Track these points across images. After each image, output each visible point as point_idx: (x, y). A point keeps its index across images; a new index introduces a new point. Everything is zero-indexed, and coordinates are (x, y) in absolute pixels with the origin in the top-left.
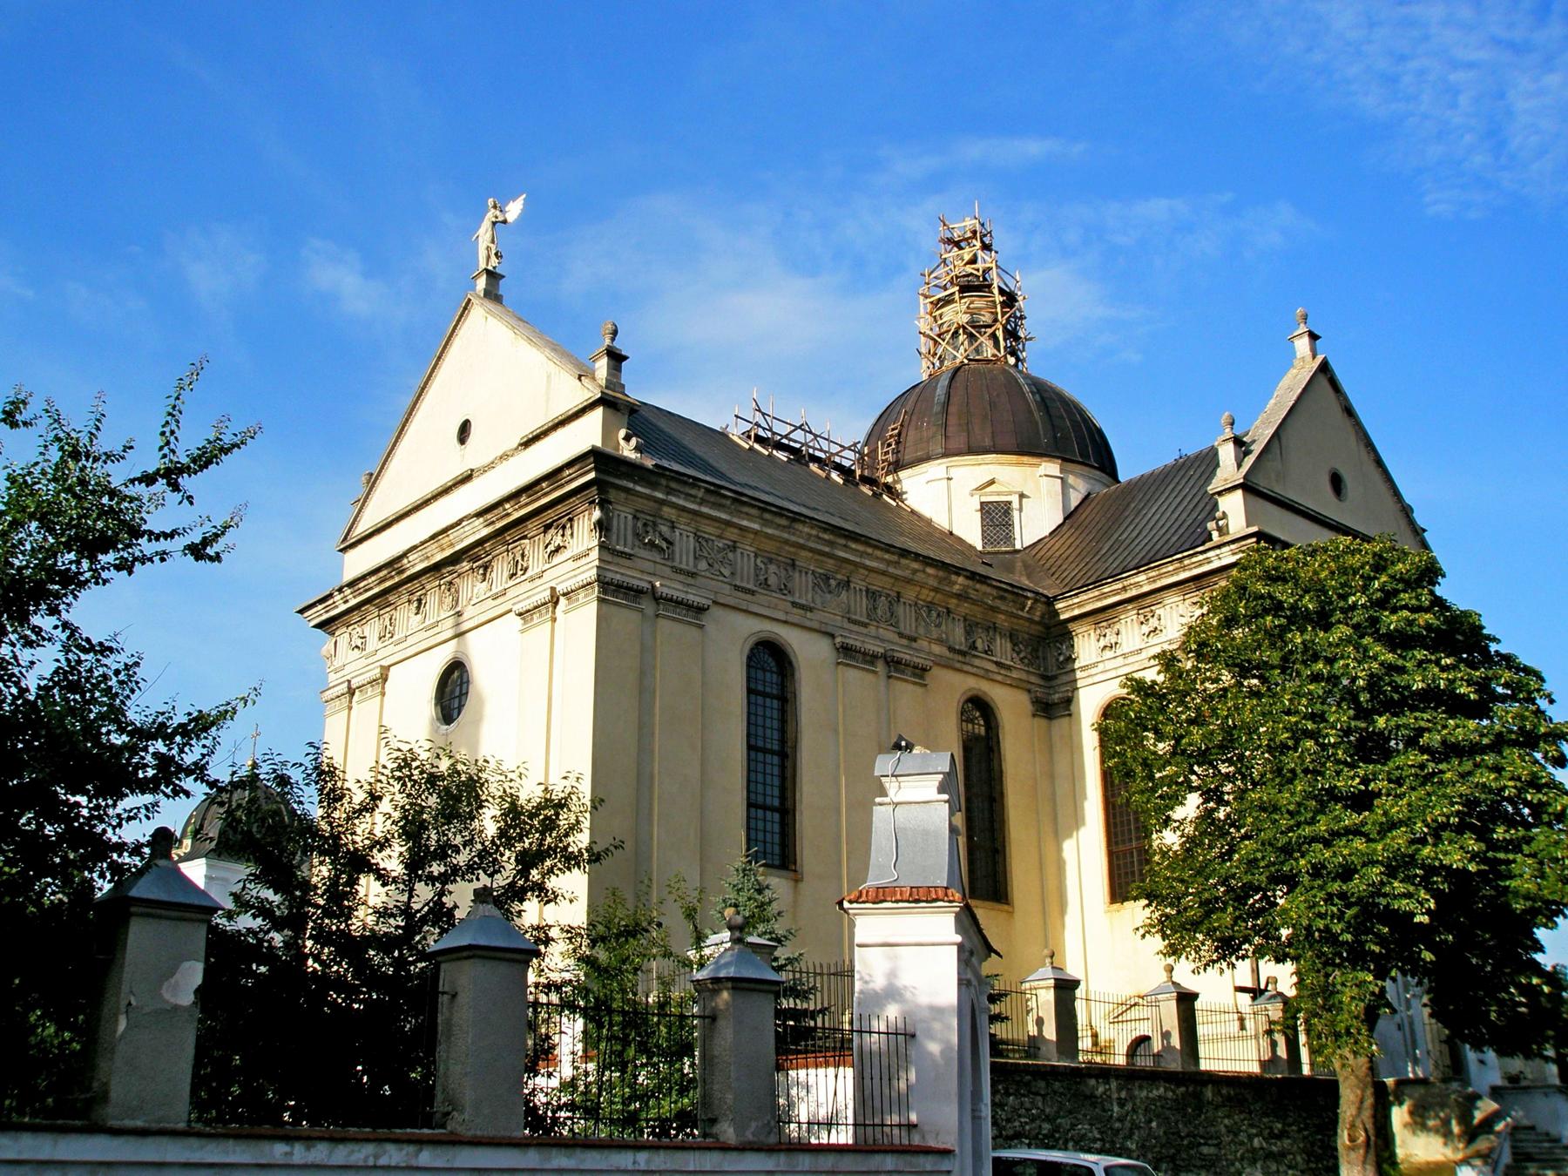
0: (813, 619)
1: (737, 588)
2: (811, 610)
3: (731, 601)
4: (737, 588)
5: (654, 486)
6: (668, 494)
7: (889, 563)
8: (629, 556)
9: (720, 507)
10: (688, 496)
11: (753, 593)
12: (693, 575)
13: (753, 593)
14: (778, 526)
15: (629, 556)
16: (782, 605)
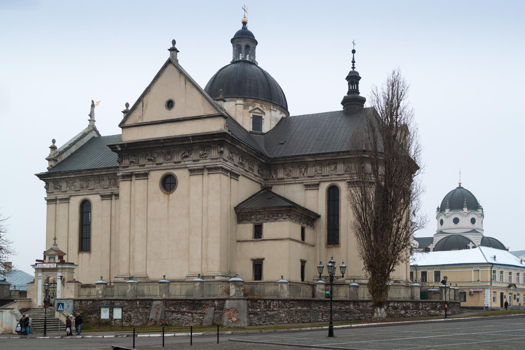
0: (94, 191)
1: (76, 191)
2: (94, 189)
3: (75, 194)
4: (76, 191)
5: (50, 177)
6: (54, 176)
7: (107, 171)
8: (52, 193)
9: (65, 175)
10: (58, 176)
11: (79, 190)
12: (66, 191)
13: (79, 190)
14: (78, 174)
15: (52, 193)
16: (86, 191)
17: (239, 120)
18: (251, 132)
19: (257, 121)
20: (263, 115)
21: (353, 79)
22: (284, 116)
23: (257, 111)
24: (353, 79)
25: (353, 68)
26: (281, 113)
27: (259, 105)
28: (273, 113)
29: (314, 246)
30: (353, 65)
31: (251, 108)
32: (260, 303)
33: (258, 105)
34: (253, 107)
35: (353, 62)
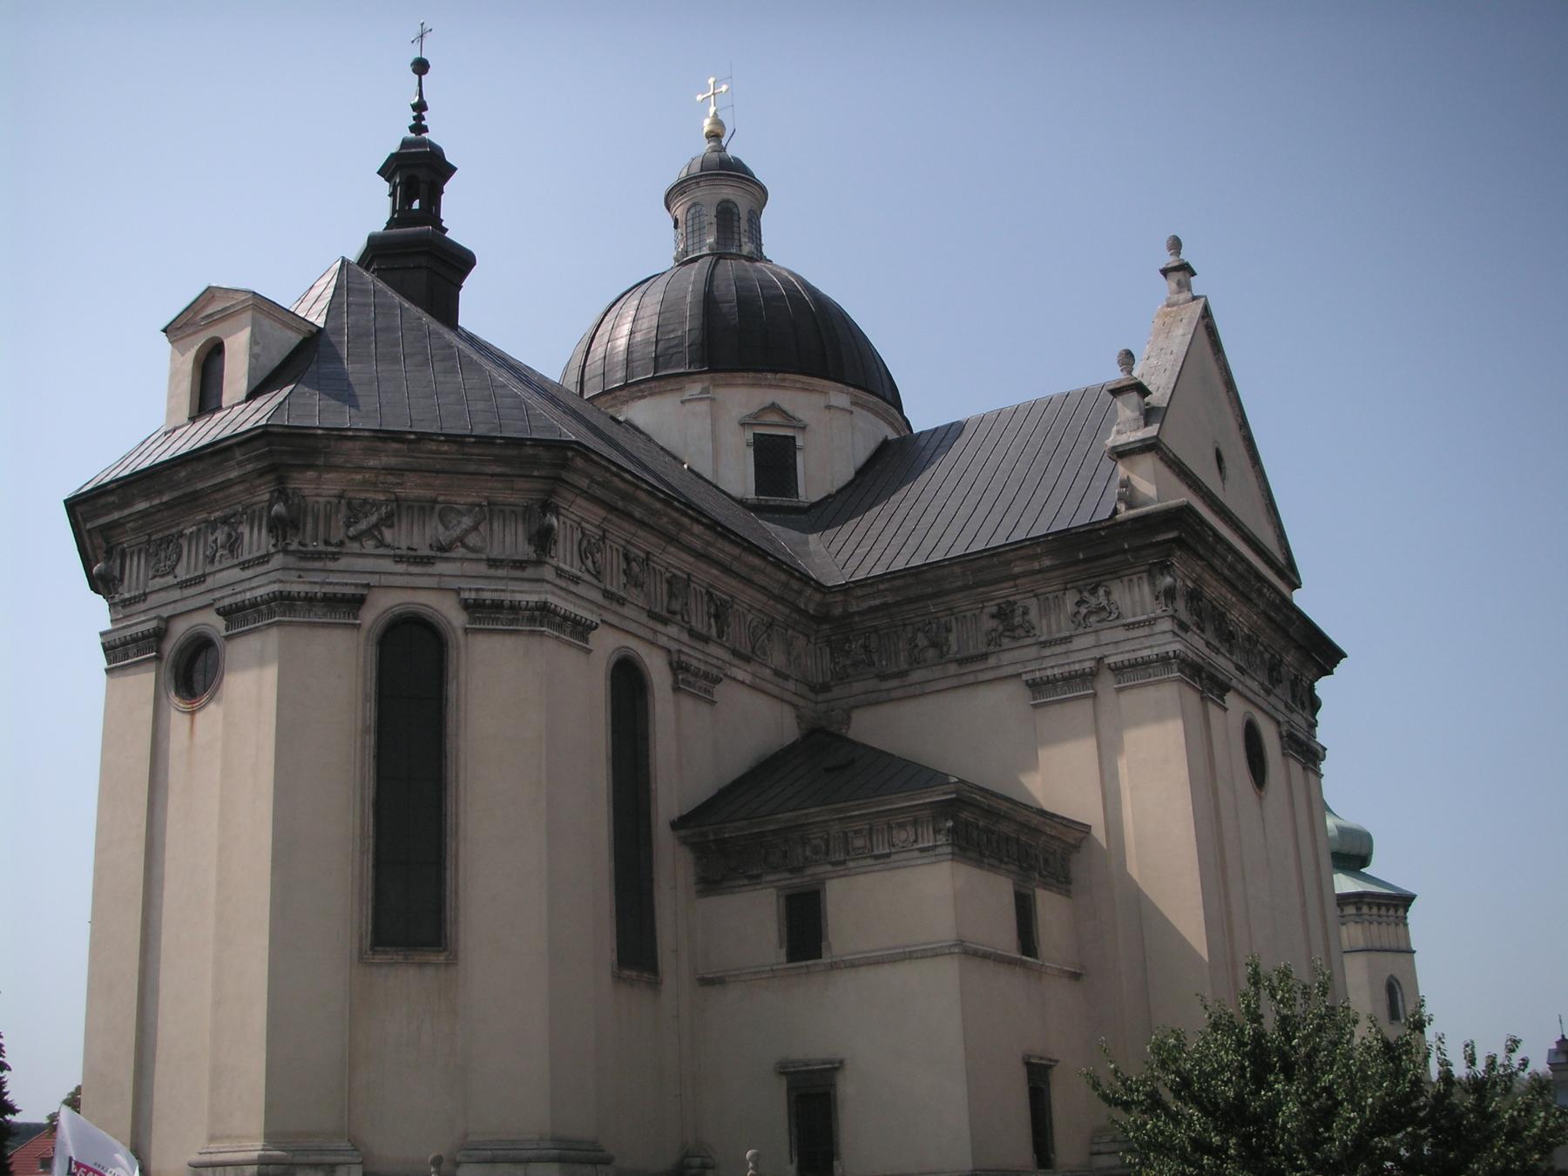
21: (418, 172)
24: (418, 172)
25: (419, 128)
30: (419, 118)
35: (420, 107)
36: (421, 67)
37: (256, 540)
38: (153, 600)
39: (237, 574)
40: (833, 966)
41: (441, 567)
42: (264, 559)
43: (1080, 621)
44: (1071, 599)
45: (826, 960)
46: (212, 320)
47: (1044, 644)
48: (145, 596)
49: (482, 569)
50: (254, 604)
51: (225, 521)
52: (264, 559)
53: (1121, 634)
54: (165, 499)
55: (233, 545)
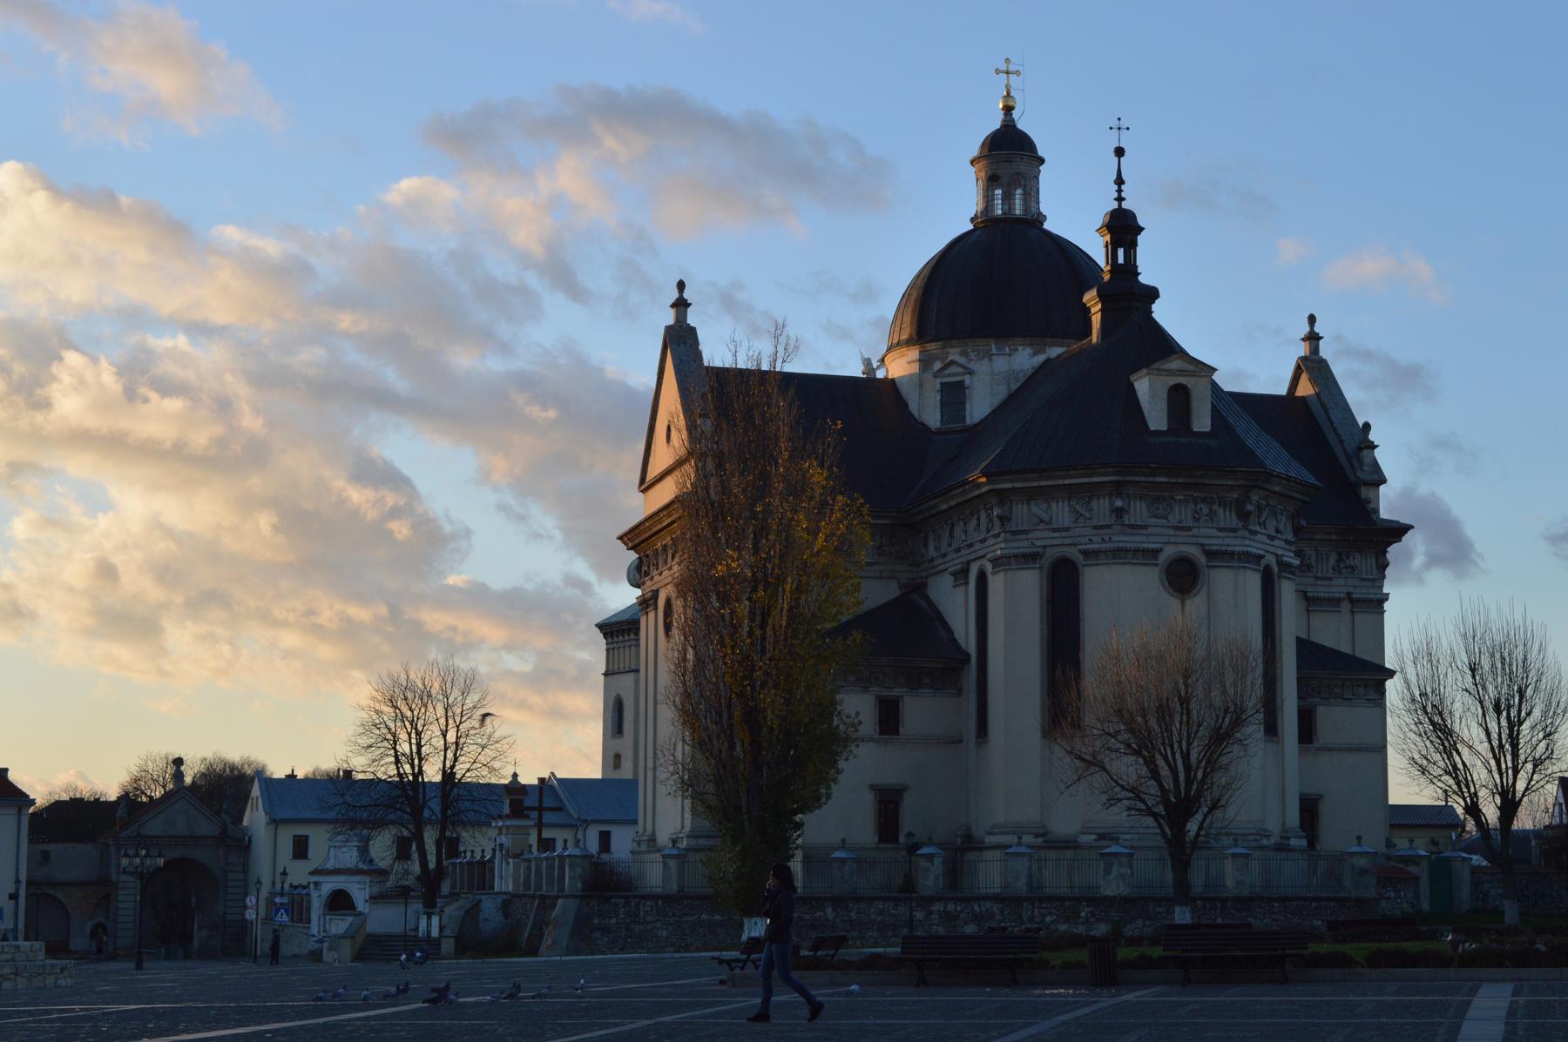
17: (914, 408)
18: (939, 432)
19: (954, 396)
20: (967, 379)
22: (1055, 352)
23: (954, 369)
24: (1122, 228)
25: (1120, 199)
26: (1035, 354)
27: (957, 350)
28: (1001, 363)
29: (961, 741)
30: (1120, 191)
31: (938, 365)
32: (616, 905)
33: (954, 354)
34: (942, 359)
35: (1120, 181)
36: (1120, 152)
37: (1227, 518)
38: (1150, 530)
39: (1214, 532)
40: (1320, 749)
41: (1277, 542)
42: (1234, 530)
43: (1337, 570)
44: (1333, 558)
45: (1316, 745)
46: (1181, 372)
47: (1317, 578)
48: (1146, 527)
49: (1282, 544)
50: (1232, 554)
51: (1204, 500)
52: (1234, 530)
53: (1357, 582)
54: (1180, 480)
55: (1212, 515)
